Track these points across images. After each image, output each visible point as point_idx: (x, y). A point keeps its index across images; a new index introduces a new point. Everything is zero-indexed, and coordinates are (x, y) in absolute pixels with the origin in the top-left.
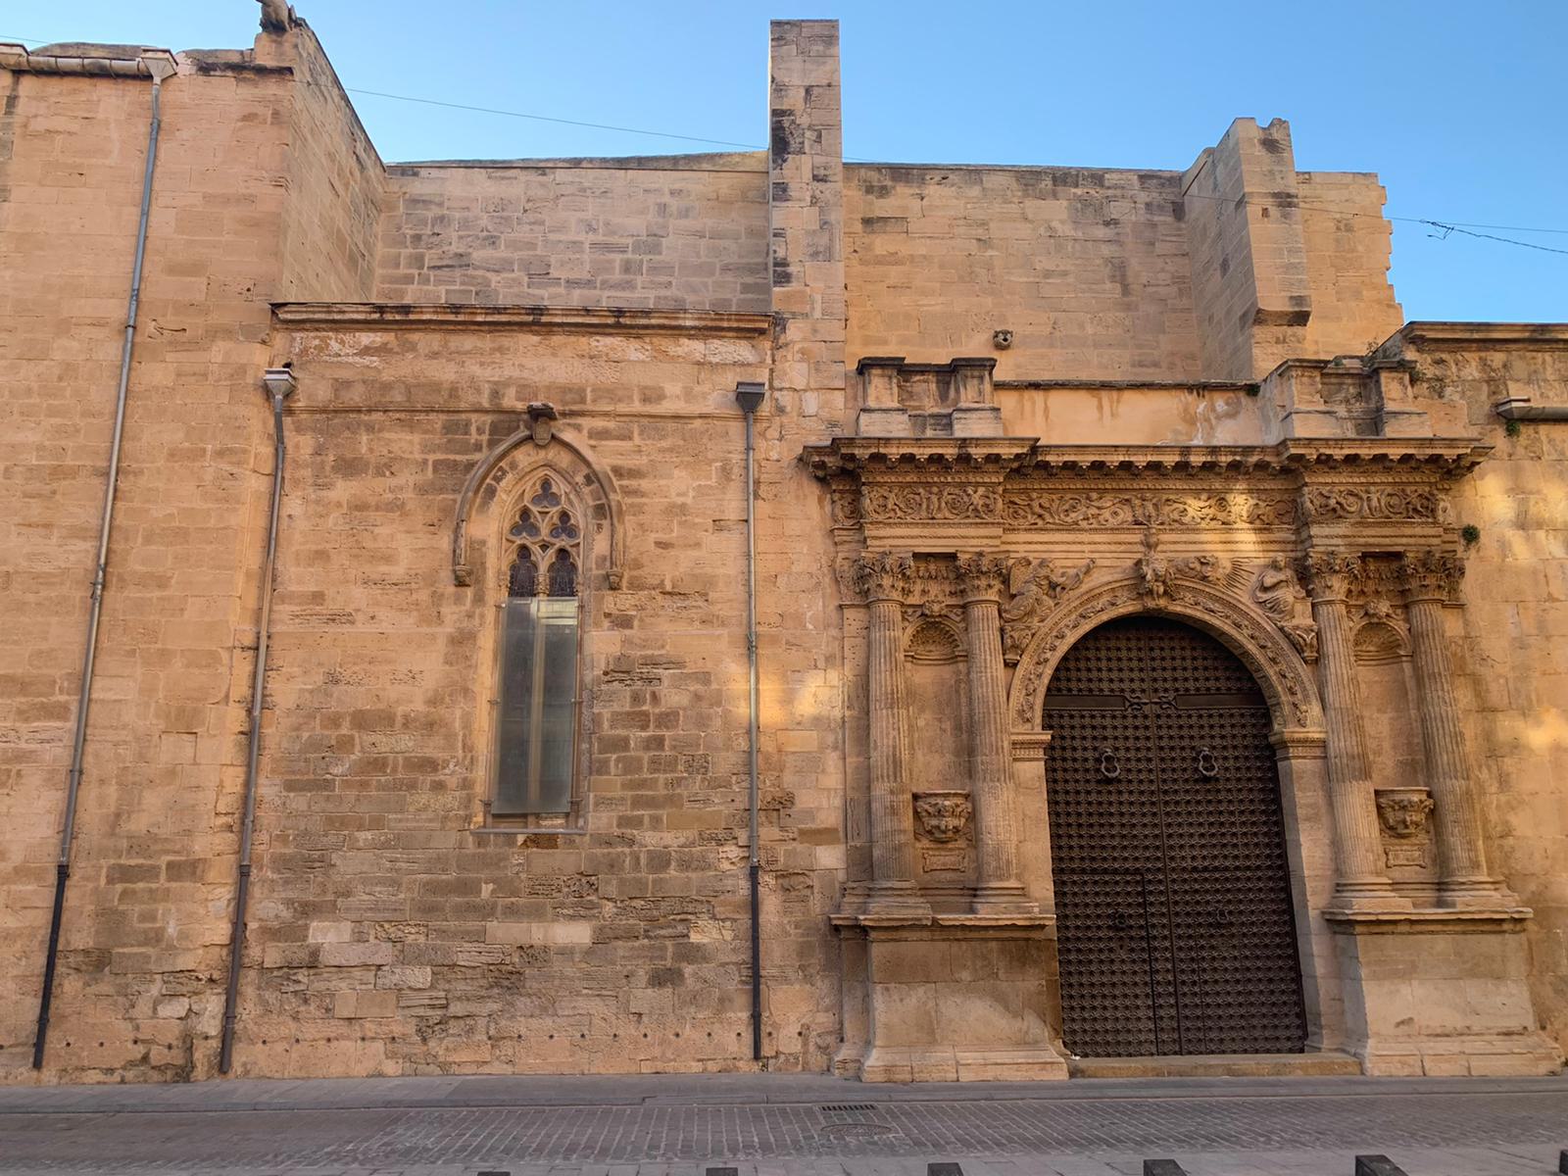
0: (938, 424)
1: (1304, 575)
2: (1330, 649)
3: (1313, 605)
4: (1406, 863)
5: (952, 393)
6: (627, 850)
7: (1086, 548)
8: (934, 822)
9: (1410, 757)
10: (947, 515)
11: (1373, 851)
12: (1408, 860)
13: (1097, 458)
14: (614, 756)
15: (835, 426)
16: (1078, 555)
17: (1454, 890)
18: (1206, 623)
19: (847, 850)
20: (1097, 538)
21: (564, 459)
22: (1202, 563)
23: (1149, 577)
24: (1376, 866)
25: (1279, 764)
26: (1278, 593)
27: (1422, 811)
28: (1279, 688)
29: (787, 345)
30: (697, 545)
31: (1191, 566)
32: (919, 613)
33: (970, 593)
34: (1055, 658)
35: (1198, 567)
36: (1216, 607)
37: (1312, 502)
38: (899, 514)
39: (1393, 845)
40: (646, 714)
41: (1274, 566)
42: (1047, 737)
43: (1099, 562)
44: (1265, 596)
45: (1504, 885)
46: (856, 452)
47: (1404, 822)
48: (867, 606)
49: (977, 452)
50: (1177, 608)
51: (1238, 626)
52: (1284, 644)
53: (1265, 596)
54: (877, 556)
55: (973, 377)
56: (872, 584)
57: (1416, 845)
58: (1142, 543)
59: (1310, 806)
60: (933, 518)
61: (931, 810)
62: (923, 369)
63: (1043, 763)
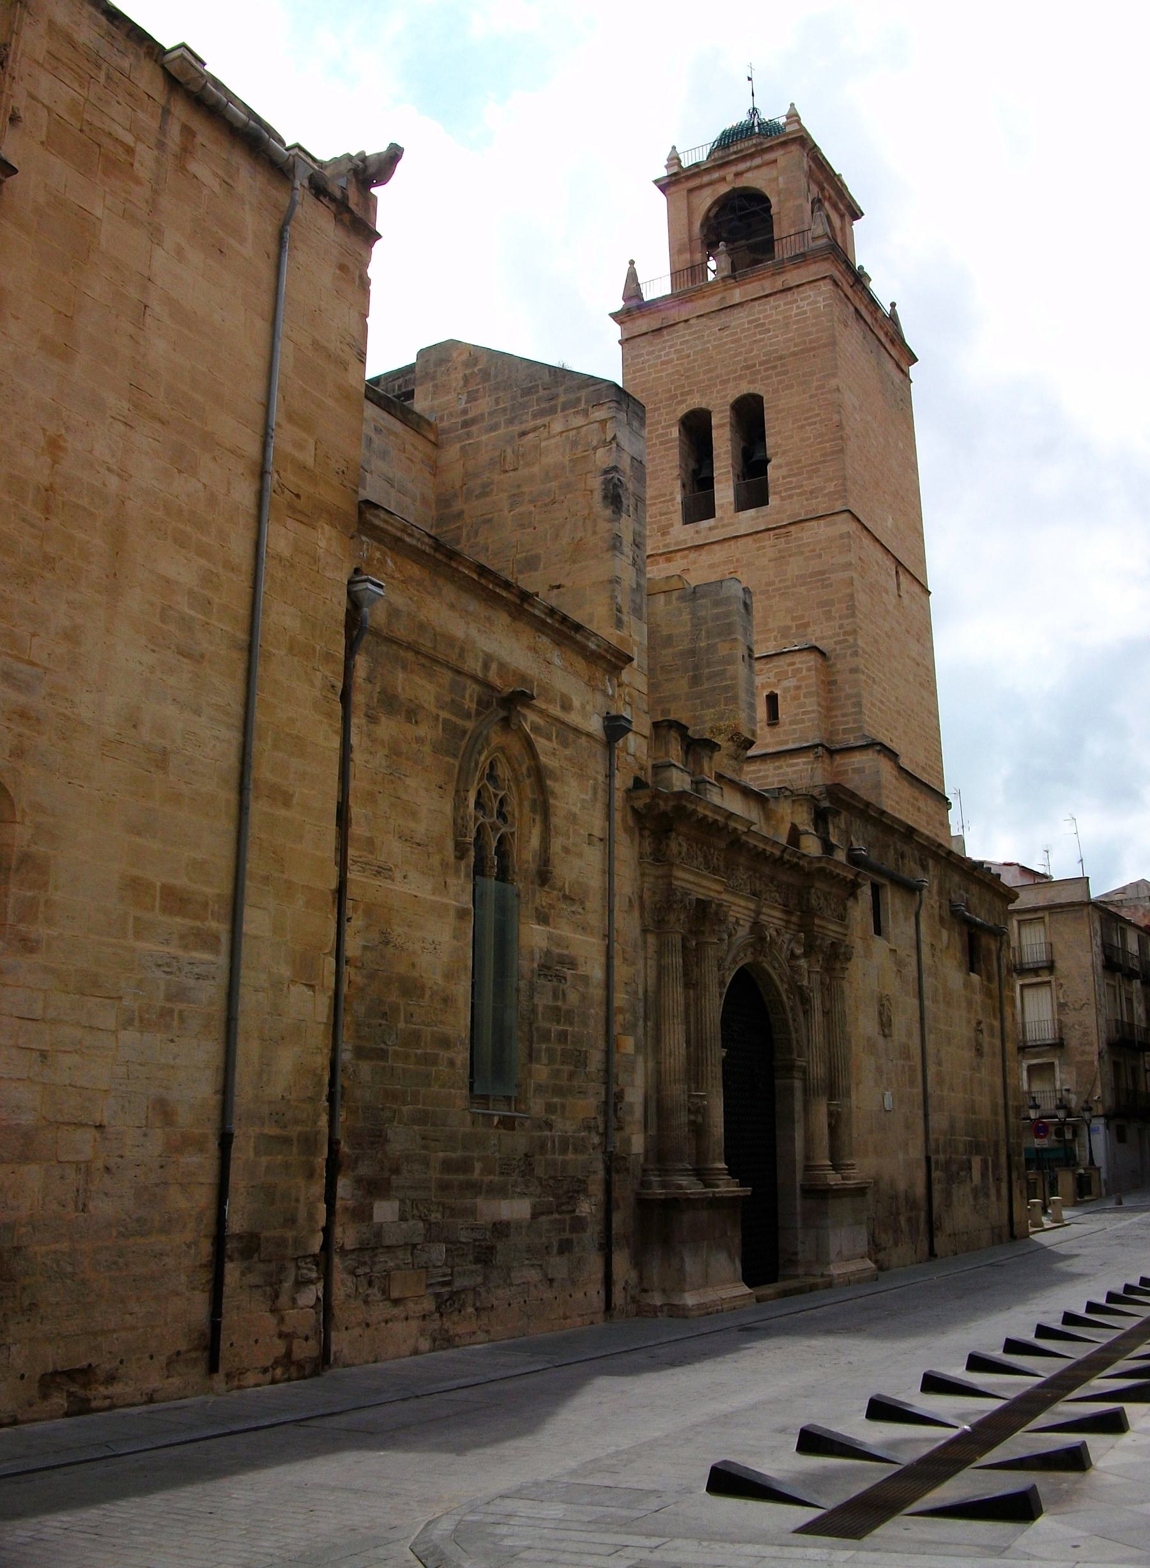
1: (810, 949)
6: (548, 1133)
14: (544, 1046)
19: (646, 1138)
21: (515, 747)
23: (768, 938)
30: (580, 855)
33: (707, 935)
40: (558, 1009)
56: (672, 917)
58: (754, 911)
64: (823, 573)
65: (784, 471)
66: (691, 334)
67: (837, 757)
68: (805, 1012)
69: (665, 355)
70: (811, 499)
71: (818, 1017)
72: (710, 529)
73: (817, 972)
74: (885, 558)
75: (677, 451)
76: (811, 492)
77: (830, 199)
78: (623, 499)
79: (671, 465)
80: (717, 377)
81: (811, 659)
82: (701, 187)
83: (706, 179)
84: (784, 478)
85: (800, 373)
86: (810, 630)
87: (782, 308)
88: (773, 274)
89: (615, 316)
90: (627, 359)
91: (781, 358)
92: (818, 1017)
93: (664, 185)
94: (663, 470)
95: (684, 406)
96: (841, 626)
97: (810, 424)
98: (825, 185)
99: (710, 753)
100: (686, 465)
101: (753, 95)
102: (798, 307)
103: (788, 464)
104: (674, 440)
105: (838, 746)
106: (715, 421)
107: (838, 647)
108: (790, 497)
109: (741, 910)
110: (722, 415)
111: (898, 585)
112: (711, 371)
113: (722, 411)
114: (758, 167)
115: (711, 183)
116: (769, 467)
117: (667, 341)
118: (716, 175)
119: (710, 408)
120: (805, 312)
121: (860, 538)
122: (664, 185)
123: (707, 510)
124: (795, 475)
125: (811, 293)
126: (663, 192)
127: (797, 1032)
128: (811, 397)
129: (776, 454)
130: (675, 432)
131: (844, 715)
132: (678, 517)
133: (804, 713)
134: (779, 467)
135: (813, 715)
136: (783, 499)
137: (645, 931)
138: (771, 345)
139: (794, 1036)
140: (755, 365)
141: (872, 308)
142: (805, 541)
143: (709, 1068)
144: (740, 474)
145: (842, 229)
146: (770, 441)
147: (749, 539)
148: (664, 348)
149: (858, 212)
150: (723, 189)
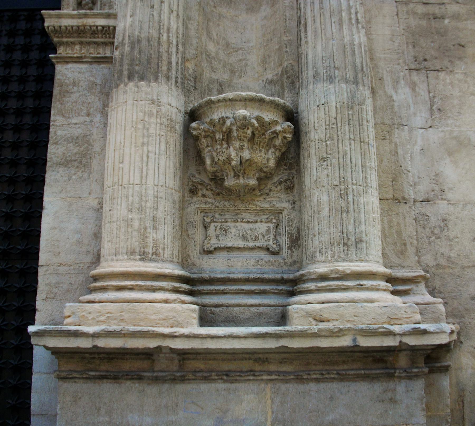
4: (240, 243)
9: (280, 70)
11: (141, 209)
12: (244, 238)
17: (309, 292)
24: (144, 237)
27: (269, 145)
39: (223, 211)
45: (422, 286)
47: (229, 160)
57: (262, 211)
59: (75, 140)
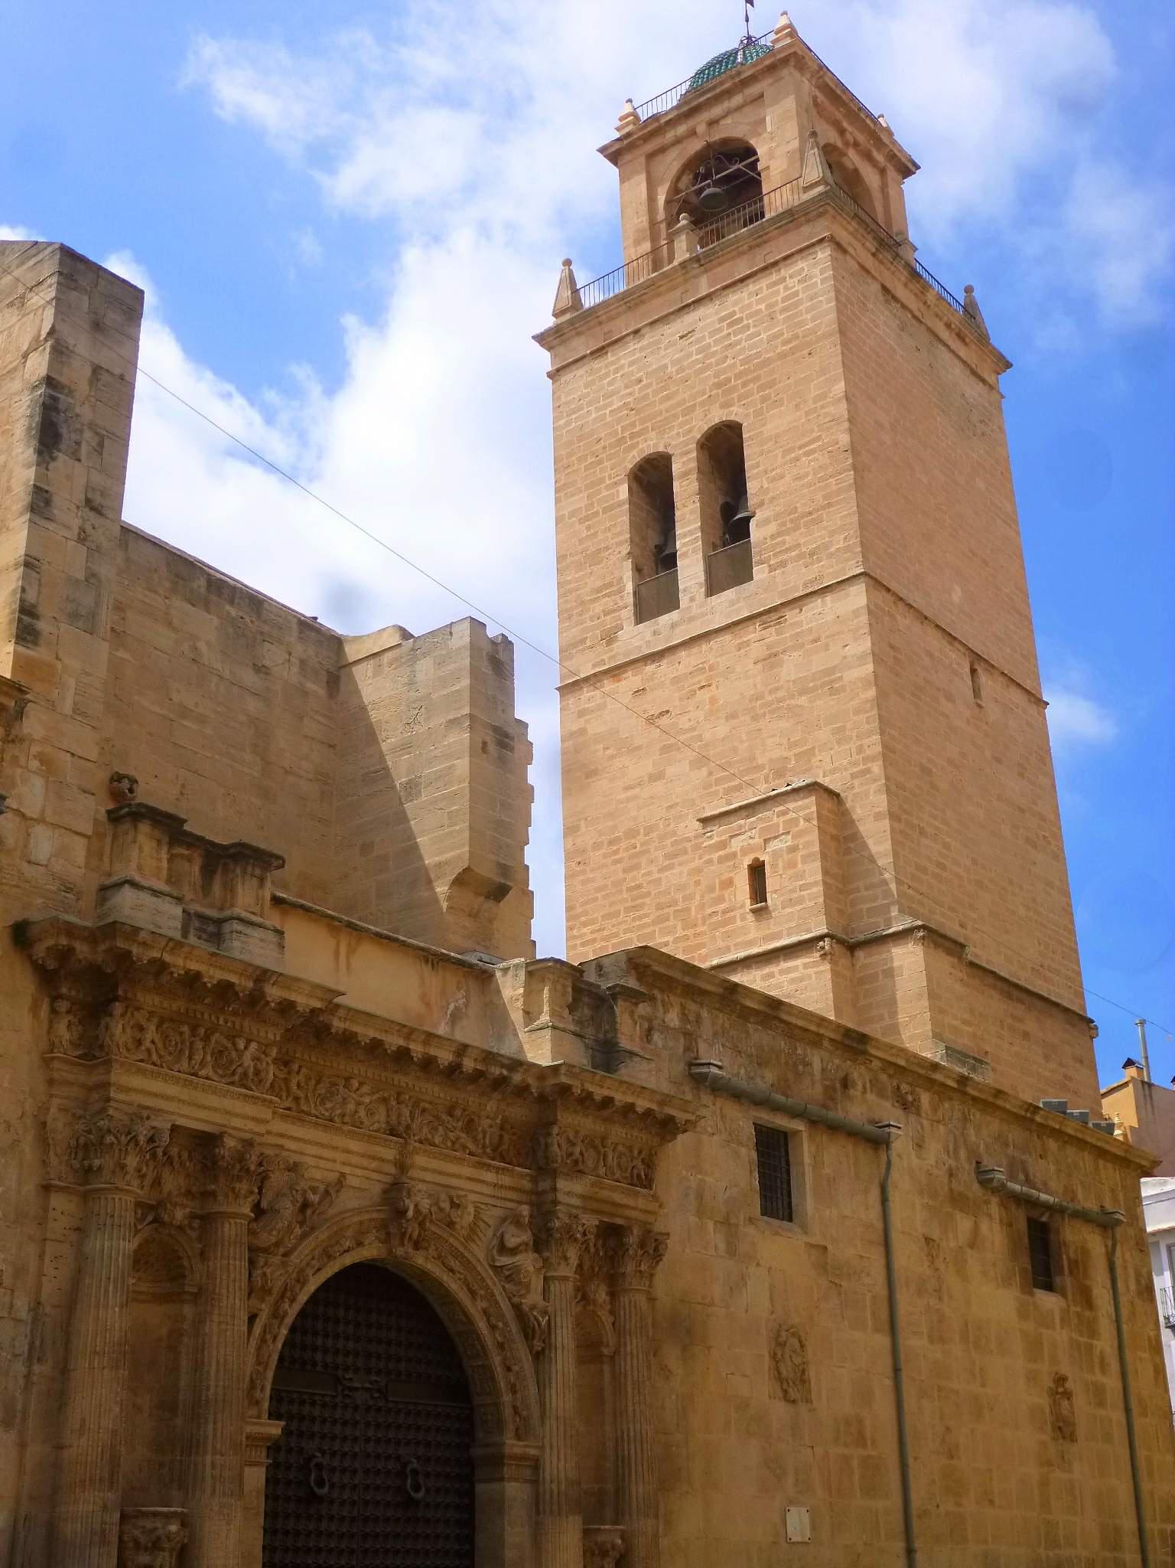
0: (204, 931)
1: (542, 1240)
2: (559, 1339)
3: (545, 1279)
5: (217, 888)
7: (340, 1156)
8: (144, 1559)
10: (211, 1074)
13: (378, 1036)
15: (69, 890)
16: (329, 1165)
18: (441, 1284)
20: (354, 1145)
22: (452, 1203)
23: (410, 1213)
25: (476, 1485)
26: (518, 1259)
28: (502, 1385)
29: (22, 740)
31: (443, 1205)
32: (150, 1218)
33: (220, 1198)
34: (292, 1311)
35: (446, 1205)
36: (455, 1264)
37: (559, 1145)
38: (155, 1057)
41: (517, 1222)
42: (275, 1429)
43: (352, 1181)
44: (504, 1260)
46: (135, 950)
48: (85, 1197)
49: (273, 993)
50: (420, 1260)
51: (473, 1294)
52: (514, 1327)
53: (504, 1260)
54: (125, 1118)
55: (253, 875)
60: (195, 1075)
61: (143, 1539)
62: (195, 842)
63: (264, 1470)
64: (830, 671)
65: (772, 528)
66: (642, 349)
67: (860, 954)
68: (538, 1357)
69: (610, 384)
70: (812, 564)
71: (564, 1363)
72: (673, 626)
73: (565, 1279)
74: (947, 648)
75: (626, 518)
76: (812, 554)
77: (856, 145)
78: (64, 430)
79: (616, 540)
80: (679, 404)
81: (809, 805)
82: (662, 150)
83: (670, 135)
84: (773, 537)
85: (791, 380)
86: (815, 761)
87: (765, 292)
88: (751, 248)
89: (542, 339)
90: (559, 398)
91: (767, 362)
92: (564, 1363)
93: (615, 153)
94: (607, 548)
95: (635, 452)
96: (860, 749)
97: (807, 454)
98: (845, 124)
99: (258, 872)
100: (644, 539)
101: (747, 20)
102: (786, 288)
103: (777, 516)
104: (620, 504)
105: (861, 937)
106: (676, 468)
107: (856, 782)
108: (783, 564)
109: (355, 1160)
110: (685, 459)
111: (977, 693)
112: (668, 398)
113: (687, 453)
114: (739, 108)
115: (678, 141)
116: (752, 524)
117: (613, 363)
118: (682, 129)
119: (670, 451)
120: (796, 294)
121: (892, 616)
122: (615, 153)
123: (669, 600)
124: (788, 532)
125: (804, 265)
126: (615, 163)
127: (513, 1390)
128: (807, 414)
129: (761, 504)
130: (623, 491)
131: (867, 889)
132: (628, 613)
133: (802, 888)
134: (767, 521)
135: (815, 890)
136: (772, 569)
137: (46, 1188)
138: (751, 348)
139: (507, 1398)
140: (728, 380)
141: (915, 286)
142: (805, 627)
143: (209, 1458)
144: (718, 542)
145: (884, 188)
146: (752, 486)
147: (727, 638)
148: (607, 375)
149: (910, 165)
150: (695, 146)
